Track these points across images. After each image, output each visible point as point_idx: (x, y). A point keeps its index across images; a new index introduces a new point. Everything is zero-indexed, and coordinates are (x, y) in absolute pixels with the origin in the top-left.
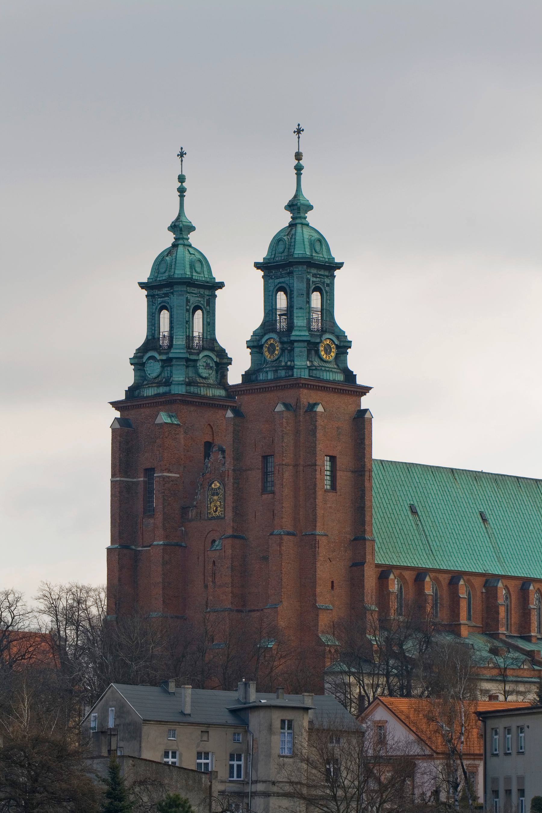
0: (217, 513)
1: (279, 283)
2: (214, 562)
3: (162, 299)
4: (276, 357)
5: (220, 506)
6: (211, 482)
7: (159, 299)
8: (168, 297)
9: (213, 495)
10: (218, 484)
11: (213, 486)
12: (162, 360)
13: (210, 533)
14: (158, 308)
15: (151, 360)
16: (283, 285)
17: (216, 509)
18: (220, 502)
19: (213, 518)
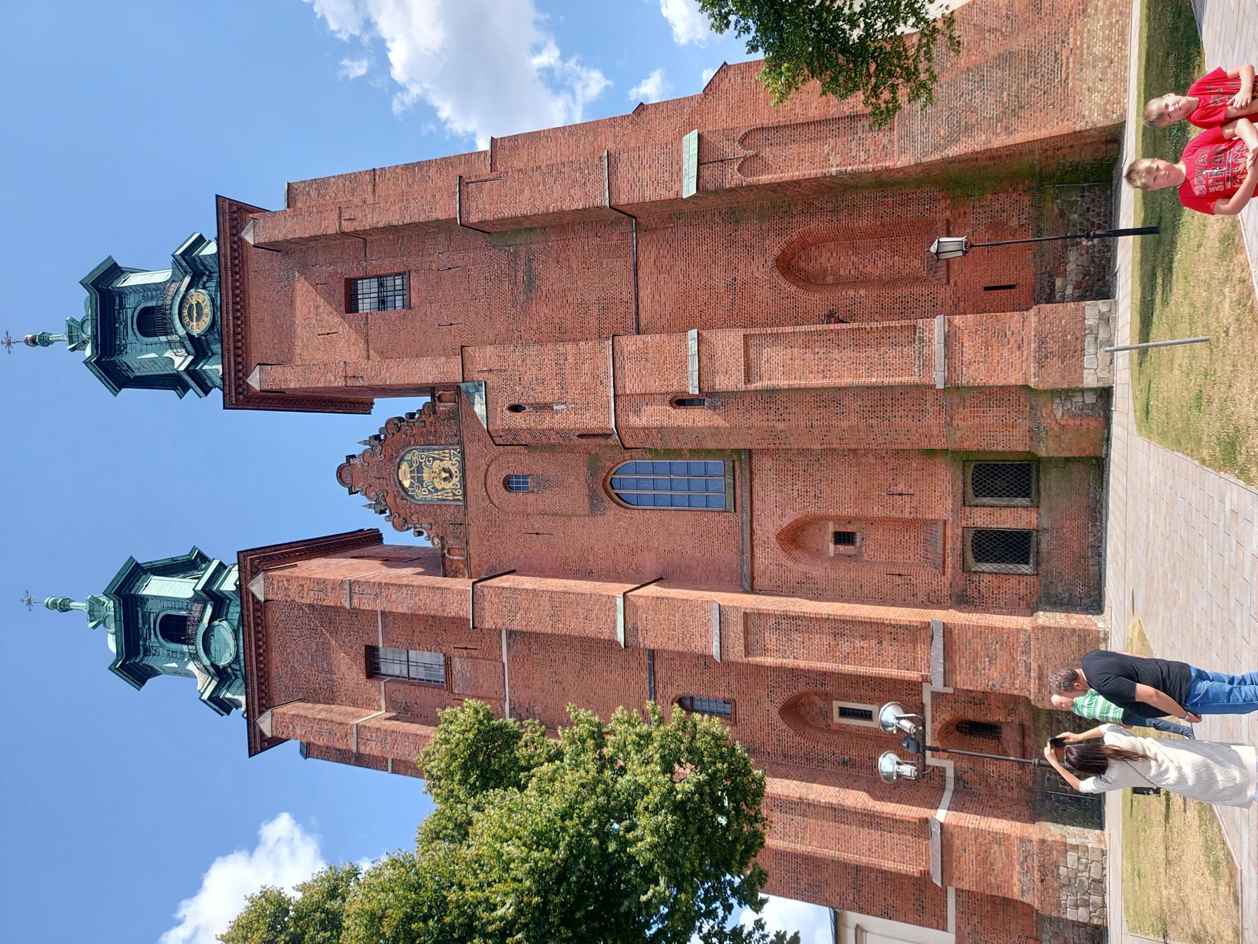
0: (454, 469)
1: (133, 329)
2: (515, 408)
3: (152, 632)
4: (207, 298)
5: (442, 460)
6: (402, 493)
7: (153, 636)
8: (150, 613)
9: (421, 480)
10: (404, 466)
11: (406, 484)
12: (212, 619)
13: (490, 494)
14: (162, 640)
15: (212, 648)
16: (135, 321)
17: (444, 470)
18: (435, 459)
19: (464, 478)
